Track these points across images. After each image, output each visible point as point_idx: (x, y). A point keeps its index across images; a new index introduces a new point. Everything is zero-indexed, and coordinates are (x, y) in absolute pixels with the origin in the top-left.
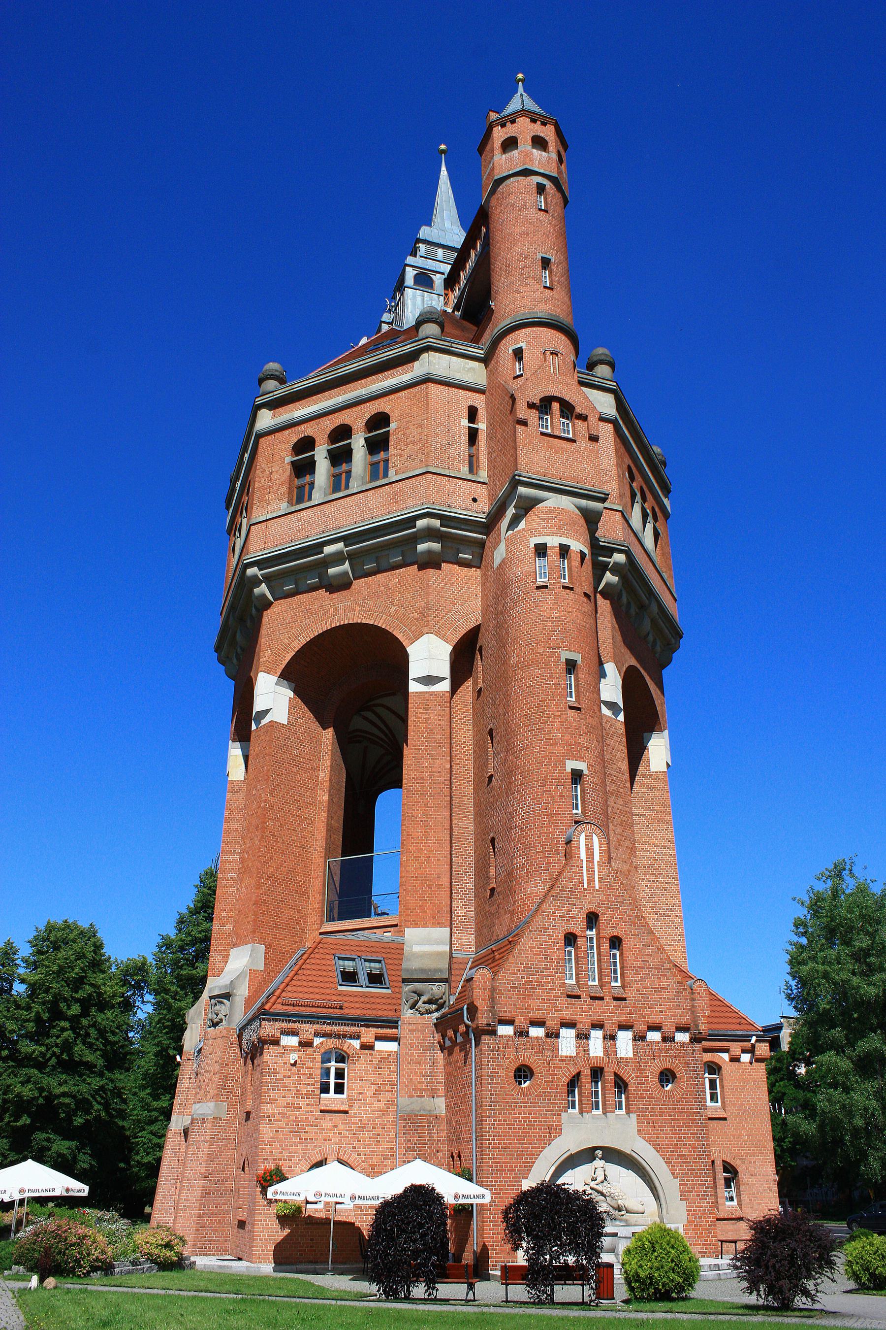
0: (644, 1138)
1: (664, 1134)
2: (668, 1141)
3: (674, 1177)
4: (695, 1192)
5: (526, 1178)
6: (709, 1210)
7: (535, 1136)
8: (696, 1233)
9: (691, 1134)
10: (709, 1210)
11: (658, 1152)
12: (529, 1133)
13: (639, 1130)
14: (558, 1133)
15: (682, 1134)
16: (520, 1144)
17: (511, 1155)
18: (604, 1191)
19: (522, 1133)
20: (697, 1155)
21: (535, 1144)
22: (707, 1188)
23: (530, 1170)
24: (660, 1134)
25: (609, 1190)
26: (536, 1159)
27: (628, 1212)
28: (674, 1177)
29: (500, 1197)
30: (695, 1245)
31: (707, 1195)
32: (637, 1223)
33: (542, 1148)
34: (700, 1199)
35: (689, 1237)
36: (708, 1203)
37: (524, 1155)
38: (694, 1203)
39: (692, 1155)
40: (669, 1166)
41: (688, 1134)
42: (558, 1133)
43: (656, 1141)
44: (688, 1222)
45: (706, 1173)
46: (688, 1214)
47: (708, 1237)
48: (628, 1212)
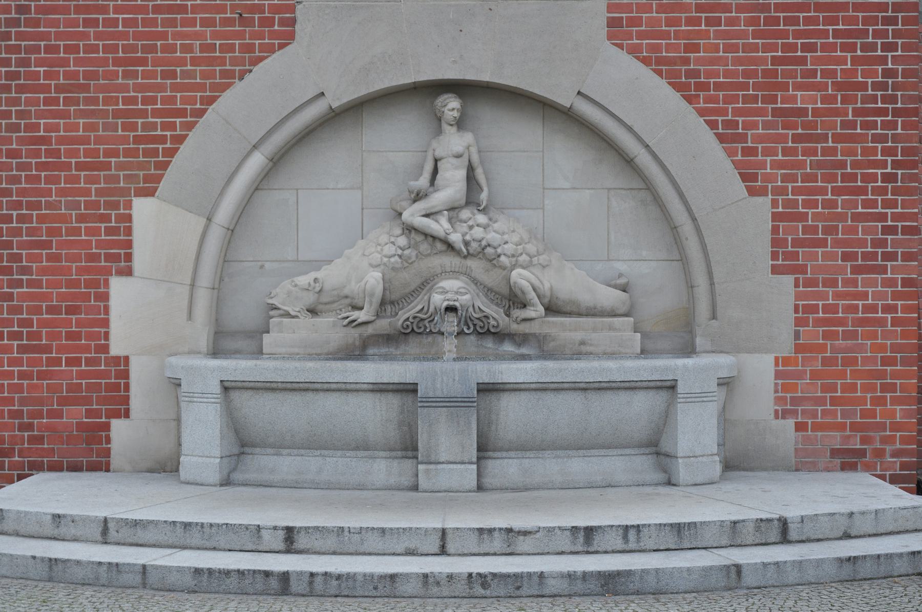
0: (633, 51)
1: (719, 35)
2: (738, 61)
3: (752, 192)
4: (837, 243)
5: (150, 193)
6: (888, 309)
7: (187, 49)
8: (826, 388)
10: (888, 309)
11: (689, 100)
12: (163, 36)
13: (613, 23)
15: (798, 34)
16: (126, 75)
18: (455, 238)
19: (138, 36)
20: (857, 112)
21: (185, 74)
22: (888, 230)
23: (164, 166)
24: (705, 35)
25: (478, 232)
26: (190, 126)
27: (552, 309)
28: (752, 192)
29: (50, 258)
30: (817, 427)
31: (889, 257)
34: (856, 270)
36: (891, 283)
37: (143, 114)
38: (833, 283)
39: (836, 112)
40: (730, 153)
43: (686, 61)
44: (799, 348)
45: (888, 178)
46: (799, 322)
47: (877, 401)
48: (552, 309)
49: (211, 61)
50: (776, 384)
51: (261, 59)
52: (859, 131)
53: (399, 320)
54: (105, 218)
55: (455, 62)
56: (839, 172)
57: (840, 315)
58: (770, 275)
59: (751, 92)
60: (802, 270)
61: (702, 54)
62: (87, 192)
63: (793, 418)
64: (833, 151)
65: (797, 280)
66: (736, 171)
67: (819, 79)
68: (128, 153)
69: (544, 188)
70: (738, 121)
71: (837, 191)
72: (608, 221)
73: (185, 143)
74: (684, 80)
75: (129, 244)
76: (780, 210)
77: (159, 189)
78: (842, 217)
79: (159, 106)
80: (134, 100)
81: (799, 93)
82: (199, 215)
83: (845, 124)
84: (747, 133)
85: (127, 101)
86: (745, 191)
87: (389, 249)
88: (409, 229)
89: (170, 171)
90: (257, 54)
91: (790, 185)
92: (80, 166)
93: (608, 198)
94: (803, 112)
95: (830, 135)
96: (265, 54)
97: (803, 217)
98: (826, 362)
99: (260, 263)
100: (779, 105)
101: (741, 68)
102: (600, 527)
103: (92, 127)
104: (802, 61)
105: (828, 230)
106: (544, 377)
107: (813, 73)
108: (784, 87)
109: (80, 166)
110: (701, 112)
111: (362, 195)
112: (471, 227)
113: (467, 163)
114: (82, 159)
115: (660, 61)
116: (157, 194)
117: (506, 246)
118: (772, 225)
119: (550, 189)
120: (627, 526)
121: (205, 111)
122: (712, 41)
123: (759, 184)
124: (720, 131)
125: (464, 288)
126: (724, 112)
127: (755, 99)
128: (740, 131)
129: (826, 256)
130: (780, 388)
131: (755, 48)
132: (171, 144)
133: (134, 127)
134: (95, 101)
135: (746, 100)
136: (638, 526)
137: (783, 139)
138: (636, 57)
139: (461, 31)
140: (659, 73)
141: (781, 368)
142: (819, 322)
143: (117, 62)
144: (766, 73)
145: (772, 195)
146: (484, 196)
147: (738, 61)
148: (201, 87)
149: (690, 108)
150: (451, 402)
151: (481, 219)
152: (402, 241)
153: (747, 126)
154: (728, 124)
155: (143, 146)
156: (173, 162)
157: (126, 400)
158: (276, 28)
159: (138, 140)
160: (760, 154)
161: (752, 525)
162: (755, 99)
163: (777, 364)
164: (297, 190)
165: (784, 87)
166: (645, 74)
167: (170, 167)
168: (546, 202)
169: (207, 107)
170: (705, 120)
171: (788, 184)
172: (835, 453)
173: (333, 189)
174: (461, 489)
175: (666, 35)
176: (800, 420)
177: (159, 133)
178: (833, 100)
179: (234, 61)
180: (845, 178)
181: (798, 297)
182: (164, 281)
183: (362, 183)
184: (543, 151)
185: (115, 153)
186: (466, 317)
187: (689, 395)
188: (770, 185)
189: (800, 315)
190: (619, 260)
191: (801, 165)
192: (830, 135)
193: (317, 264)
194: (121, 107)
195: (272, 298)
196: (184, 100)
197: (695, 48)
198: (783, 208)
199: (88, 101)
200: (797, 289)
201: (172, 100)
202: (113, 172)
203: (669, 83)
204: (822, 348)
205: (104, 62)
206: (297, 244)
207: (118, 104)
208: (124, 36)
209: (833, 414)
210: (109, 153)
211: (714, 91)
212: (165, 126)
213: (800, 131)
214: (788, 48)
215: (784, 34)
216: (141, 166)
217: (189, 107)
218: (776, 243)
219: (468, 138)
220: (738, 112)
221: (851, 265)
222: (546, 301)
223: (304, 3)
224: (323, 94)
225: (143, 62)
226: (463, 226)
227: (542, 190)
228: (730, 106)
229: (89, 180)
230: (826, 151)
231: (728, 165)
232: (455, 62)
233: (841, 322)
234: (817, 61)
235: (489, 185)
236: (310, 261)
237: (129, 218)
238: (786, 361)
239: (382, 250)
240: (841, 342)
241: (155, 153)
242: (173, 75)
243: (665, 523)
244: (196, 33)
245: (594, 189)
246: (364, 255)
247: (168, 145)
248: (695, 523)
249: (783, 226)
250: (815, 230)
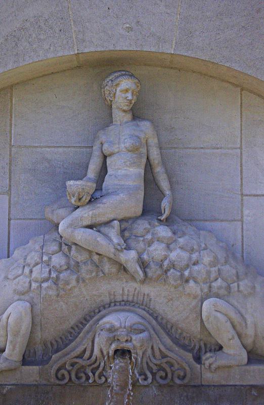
55: (130, 29)
69: (242, 195)
88: (65, 245)
111: (10, 200)
112: (150, 243)
113: (144, 160)
117: (196, 268)
119: (250, 195)
146: (165, 204)
151: (163, 232)
152: (58, 260)
168: (246, 212)
184: (241, 148)
219: (146, 126)
222: (249, 341)
227: (240, 197)
232: (130, 29)
235: (172, 189)
239: (31, 272)
246: (8, 279)
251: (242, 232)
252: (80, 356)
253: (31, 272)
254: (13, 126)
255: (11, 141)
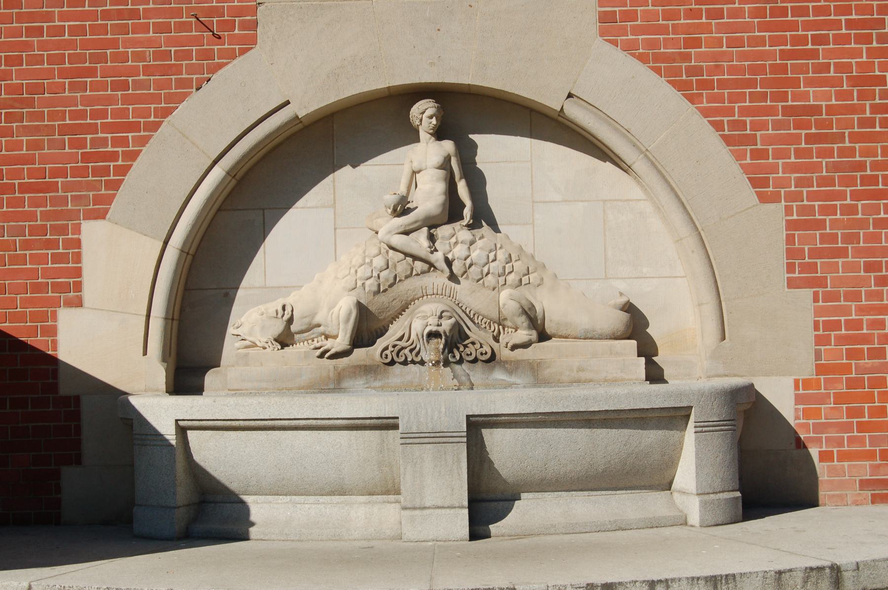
0: (629, 48)
1: (721, 28)
2: (744, 56)
3: (764, 198)
4: (859, 252)
5: (101, 215)
7: (139, 57)
8: (852, 413)
9: (850, 24)
11: (691, 99)
12: (114, 44)
13: (605, 18)
14: (242, 40)
15: (808, 26)
16: (73, 87)
17: (37, 130)
19: (85, 45)
21: (138, 85)
23: (115, 186)
24: (707, 29)
26: (144, 141)
30: (844, 456)
32: (583, 375)
33: (170, 98)
35: (819, 428)
37: (93, 129)
38: (856, 297)
39: (852, 109)
40: (739, 156)
41: (837, 25)
42: (242, 40)
44: (821, 369)
46: (820, 340)
49: (166, 70)
50: (796, 410)
51: (221, 66)
52: (878, 129)
53: (376, 349)
54: (53, 244)
55: (432, 64)
56: (858, 174)
57: (865, 331)
58: (786, 290)
59: (759, 90)
60: (820, 282)
61: (703, 49)
62: (32, 216)
63: (817, 448)
64: (851, 152)
65: (816, 295)
66: (745, 176)
67: (832, 74)
68: (76, 172)
69: (533, 202)
70: (745, 122)
71: (856, 196)
72: (605, 235)
73: (139, 159)
74: (684, 77)
75: (78, 272)
76: (795, 217)
77: (110, 211)
78: (863, 224)
79: (109, 120)
80: (82, 115)
81: (811, 90)
82: (154, 238)
83: (863, 123)
84: (756, 134)
85: (75, 115)
86: (756, 197)
87: (364, 272)
89: (122, 190)
90: (216, 61)
91: (805, 190)
92: (24, 188)
93: (604, 211)
94: (815, 110)
95: (847, 134)
96: (225, 61)
97: (821, 225)
98: (851, 383)
99: (224, 291)
100: (790, 103)
101: (746, 63)
102: (620, 584)
103: (37, 146)
104: (814, 54)
105: (848, 238)
106: (543, 406)
107: (826, 68)
108: (795, 83)
109: (24, 188)
110: (705, 113)
114: (26, 180)
115: (657, 58)
116: (108, 216)
118: (787, 234)
120: (653, 581)
121: (160, 123)
122: (714, 35)
123: (771, 189)
124: (726, 132)
125: (447, 311)
126: (730, 112)
127: (763, 97)
128: (748, 132)
129: (848, 267)
130: (801, 413)
131: (761, 41)
132: (123, 161)
133: (82, 144)
134: (40, 116)
135: (753, 97)
136: (667, 580)
137: (796, 139)
138: (631, 54)
139: (439, 30)
140: (657, 71)
141: (801, 391)
142: (841, 340)
143: (63, 74)
144: (775, 69)
145: (785, 202)
147: (744, 56)
148: (156, 99)
149: (691, 108)
150: (437, 437)
153: (756, 127)
154: (734, 125)
155: (92, 164)
156: (125, 181)
157: (78, 444)
158: (236, 31)
159: (86, 157)
160: (770, 157)
161: (801, 574)
162: (763, 97)
163: (797, 387)
164: (263, 210)
165: (795, 83)
166: (643, 74)
167: (122, 186)
169: (162, 120)
170: (709, 121)
171: (802, 189)
172: (865, 484)
173: (302, 208)
174: (451, 538)
175: (664, 30)
176: (824, 449)
177: (110, 149)
178: (848, 95)
179: (191, 70)
180: (866, 180)
181: (818, 312)
182: (117, 312)
183: (334, 200)
185: (63, 173)
186: (451, 343)
187: (706, 424)
188: (783, 191)
189: (821, 332)
190: (618, 278)
191: (817, 167)
192: (847, 134)
193: (288, 289)
194: (68, 122)
195: (238, 328)
196: (138, 113)
197: (697, 43)
198: (797, 216)
199: (33, 116)
200: (816, 304)
201: (124, 113)
202: (60, 193)
203: (669, 82)
204: (847, 369)
205: (49, 74)
206: (265, 268)
207: (64, 120)
208: (71, 44)
209: (861, 441)
210: (56, 173)
211: (717, 89)
212: (116, 142)
213: (813, 131)
214: (797, 40)
215: (793, 26)
216: (90, 186)
217: (142, 120)
218: (792, 253)
220: (744, 111)
221: (875, 277)
223: (266, 4)
224: (287, 103)
225: (92, 72)
226: (446, 244)
228: (737, 105)
229: (35, 203)
230: (842, 152)
231: (734, 168)
232: (432, 64)
233: (866, 339)
234: (829, 54)
236: (278, 287)
237: (78, 243)
238: (807, 384)
239: (356, 272)
240: (866, 361)
241: (106, 171)
242: (125, 86)
243: (698, 575)
244: (149, 40)
245: (587, 201)
246: (338, 278)
247: (120, 163)
248: (734, 576)
249: (798, 234)
250: (833, 238)
251: (534, 233)
252: (401, 339)
253: (356, 272)
254: (335, 148)
255: (333, 162)
